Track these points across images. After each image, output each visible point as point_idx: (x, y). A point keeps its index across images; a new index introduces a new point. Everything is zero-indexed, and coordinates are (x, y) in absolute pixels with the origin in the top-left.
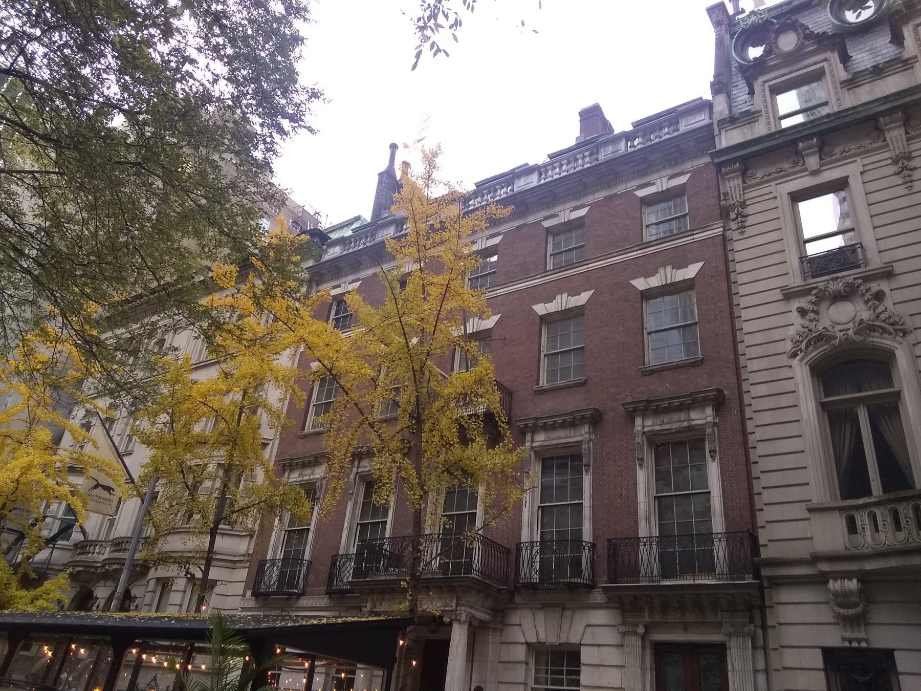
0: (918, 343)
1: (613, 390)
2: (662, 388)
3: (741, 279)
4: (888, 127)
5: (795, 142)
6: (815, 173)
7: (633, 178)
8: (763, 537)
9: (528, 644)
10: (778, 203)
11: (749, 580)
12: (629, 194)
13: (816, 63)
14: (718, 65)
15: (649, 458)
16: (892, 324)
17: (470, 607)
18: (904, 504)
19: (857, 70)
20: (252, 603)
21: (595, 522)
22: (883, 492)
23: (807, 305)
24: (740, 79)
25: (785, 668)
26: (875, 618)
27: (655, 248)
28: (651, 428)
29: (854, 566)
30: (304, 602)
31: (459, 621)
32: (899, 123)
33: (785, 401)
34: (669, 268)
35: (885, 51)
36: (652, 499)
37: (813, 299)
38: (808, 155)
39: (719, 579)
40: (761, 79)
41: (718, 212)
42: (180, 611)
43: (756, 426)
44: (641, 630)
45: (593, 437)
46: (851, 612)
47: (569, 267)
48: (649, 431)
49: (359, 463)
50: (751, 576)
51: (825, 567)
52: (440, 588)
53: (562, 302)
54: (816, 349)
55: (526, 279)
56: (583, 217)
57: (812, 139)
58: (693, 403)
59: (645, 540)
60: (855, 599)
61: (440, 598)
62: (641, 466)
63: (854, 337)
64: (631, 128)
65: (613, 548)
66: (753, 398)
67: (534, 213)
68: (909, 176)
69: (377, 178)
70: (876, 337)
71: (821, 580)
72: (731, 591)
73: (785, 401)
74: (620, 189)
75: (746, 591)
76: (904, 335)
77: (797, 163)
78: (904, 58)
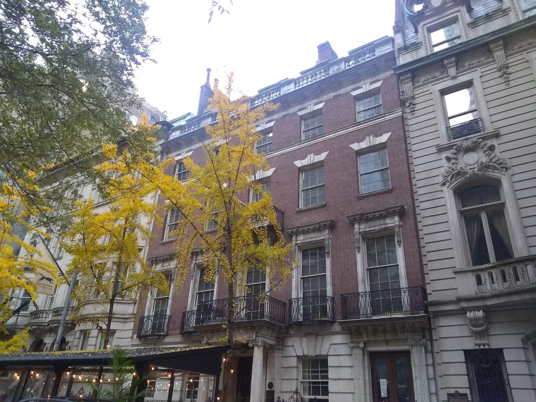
0: (514, 174)
1: (341, 209)
2: (369, 206)
3: (413, 141)
4: (495, 49)
5: (442, 60)
6: (454, 78)
7: (350, 85)
8: (429, 290)
9: (297, 356)
10: (433, 96)
11: (422, 314)
12: (347, 94)
13: (452, 13)
14: (397, 16)
15: (363, 247)
16: (499, 164)
17: (264, 337)
18: (508, 266)
19: (477, 17)
20: (137, 342)
21: (333, 285)
22: (497, 260)
23: (450, 155)
24: (410, 24)
25: (443, 363)
26: (492, 332)
27: (364, 125)
28: (363, 230)
29: (481, 303)
30: (168, 340)
31: (258, 346)
32: (501, 47)
33: (439, 211)
34: (372, 137)
35: (492, 5)
36: (366, 270)
37: (454, 151)
38: (450, 67)
39: (405, 314)
40: (422, 24)
41: (399, 103)
42: (95, 349)
43: (424, 226)
44: (362, 345)
45: (331, 236)
46: (479, 329)
47: (314, 138)
48: (362, 232)
49: (196, 258)
50: (423, 311)
51: (464, 305)
52: (246, 327)
53: (311, 159)
54: (456, 180)
55: (289, 146)
56: (321, 109)
57: (452, 58)
58: (387, 214)
59: (362, 294)
60: (481, 322)
62: (359, 251)
63: (478, 172)
64: (348, 55)
65: (344, 299)
66: (421, 210)
67: (293, 107)
68: (507, 78)
69: (200, 89)
70: (491, 172)
71: (463, 312)
72: (412, 321)
73: (439, 211)
74: (342, 91)
75: (420, 320)
76: (506, 170)
77: (444, 72)
78: (503, 9)
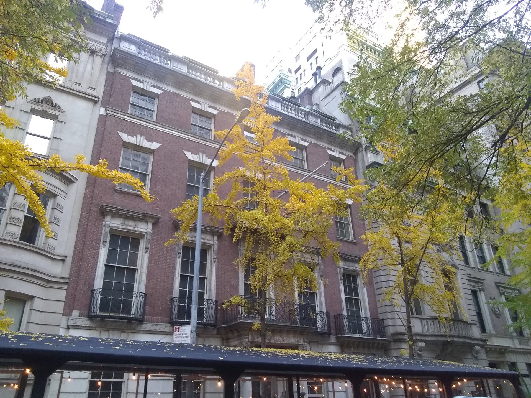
30: (146, 326)
51: (418, 338)
61: (294, 337)
67: (283, 127)
